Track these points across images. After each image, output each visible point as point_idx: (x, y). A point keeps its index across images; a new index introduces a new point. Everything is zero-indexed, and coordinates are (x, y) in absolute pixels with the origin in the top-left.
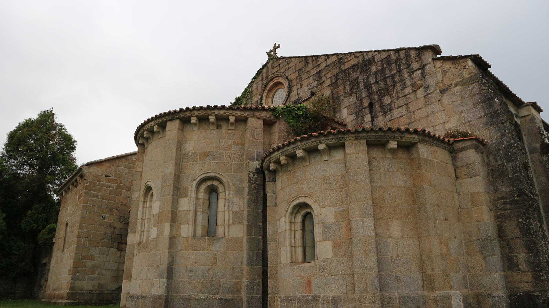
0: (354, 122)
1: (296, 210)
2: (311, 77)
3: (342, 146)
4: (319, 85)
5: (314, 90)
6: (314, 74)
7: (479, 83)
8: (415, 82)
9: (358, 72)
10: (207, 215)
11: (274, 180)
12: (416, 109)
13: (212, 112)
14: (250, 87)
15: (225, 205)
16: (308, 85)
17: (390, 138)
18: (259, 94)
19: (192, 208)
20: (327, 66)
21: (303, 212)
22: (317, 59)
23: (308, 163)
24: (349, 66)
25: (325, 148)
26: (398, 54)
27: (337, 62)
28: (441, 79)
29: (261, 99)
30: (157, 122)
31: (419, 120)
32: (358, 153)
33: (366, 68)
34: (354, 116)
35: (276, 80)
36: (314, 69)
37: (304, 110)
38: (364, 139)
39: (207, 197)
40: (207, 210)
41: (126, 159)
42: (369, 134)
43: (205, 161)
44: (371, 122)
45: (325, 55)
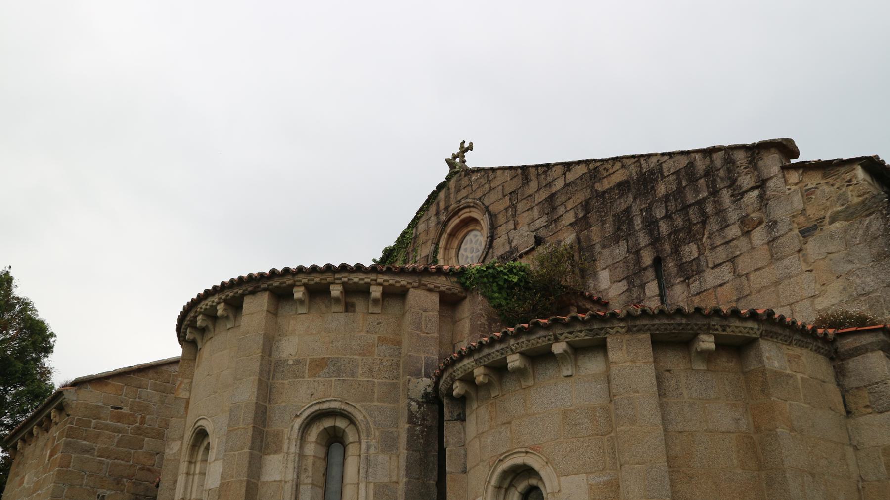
0: (624, 297)
1: (508, 480)
2: (536, 208)
3: (601, 347)
4: (551, 223)
5: (542, 233)
6: (540, 200)
7: (882, 214)
8: (748, 215)
9: (630, 195)
10: (320, 492)
11: (462, 418)
12: (752, 269)
13: (337, 276)
14: (413, 228)
15: (359, 470)
16: (529, 224)
17: (700, 329)
19: (290, 476)
20: (566, 185)
21: (522, 486)
22: (547, 171)
23: (531, 383)
24: (611, 185)
25: (565, 351)
26: (711, 158)
27: (588, 176)
28: (801, 206)
29: (436, 252)
30: (224, 297)
31: (759, 291)
32: (633, 361)
33: (646, 187)
34: (623, 286)
35: (464, 214)
37: (522, 273)
38: (645, 332)
39: (322, 453)
40: (320, 480)
41: (157, 373)
42: (656, 322)
43: (319, 377)
44: (659, 298)
45: (562, 164)
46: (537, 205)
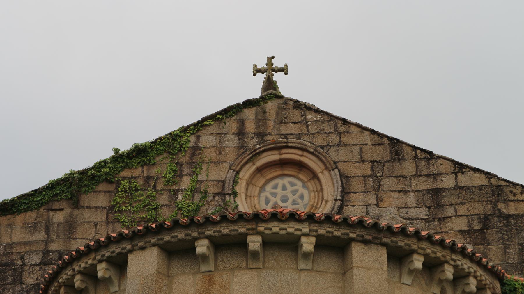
4: (434, 220)
13: (454, 257)
16: (399, 208)
18: (226, 166)
20: (457, 187)
30: (322, 232)
36: (421, 179)
46: (413, 191)
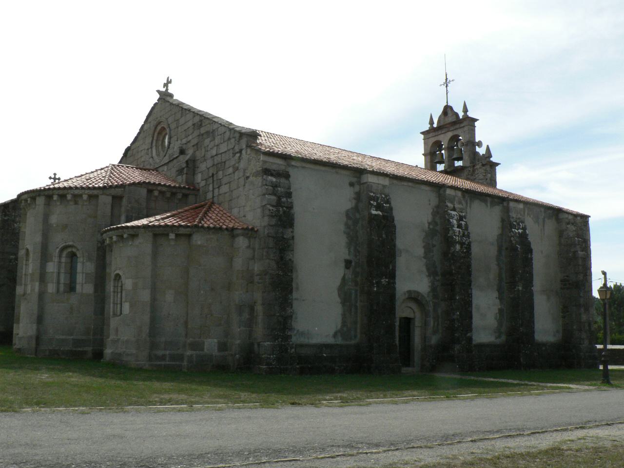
5: (184, 147)
19: (56, 270)
